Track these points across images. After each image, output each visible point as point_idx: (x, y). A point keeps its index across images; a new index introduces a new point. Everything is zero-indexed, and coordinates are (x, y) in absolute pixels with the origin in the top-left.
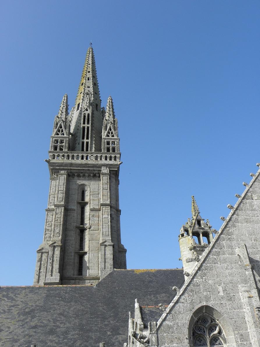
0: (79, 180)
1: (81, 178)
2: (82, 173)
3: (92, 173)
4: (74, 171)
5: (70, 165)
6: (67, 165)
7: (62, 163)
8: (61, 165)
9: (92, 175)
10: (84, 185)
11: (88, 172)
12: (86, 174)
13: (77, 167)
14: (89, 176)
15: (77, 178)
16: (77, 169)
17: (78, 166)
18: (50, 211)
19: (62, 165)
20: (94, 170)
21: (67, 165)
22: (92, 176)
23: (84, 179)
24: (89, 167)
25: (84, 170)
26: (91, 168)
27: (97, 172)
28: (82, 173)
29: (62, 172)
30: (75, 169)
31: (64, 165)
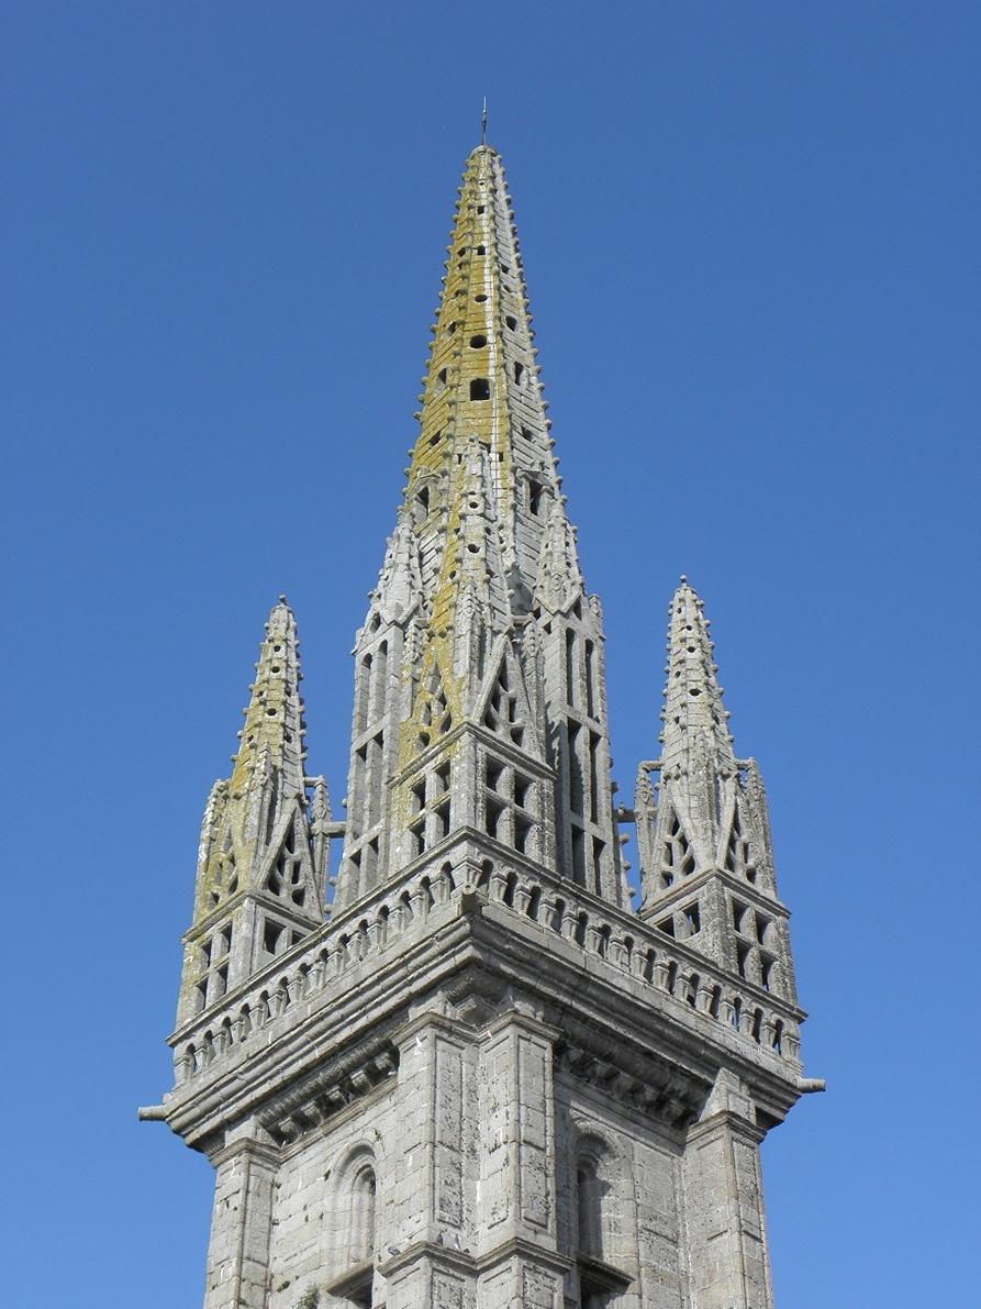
0: (582, 1097)
1: (587, 1091)
2: (608, 1058)
3: (652, 1085)
4: (579, 1030)
5: (575, 982)
6: (561, 974)
7: (542, 952)
8: (533, 958)
9: (650, 1093)
10: (594, 1145)
11: (641, 1065)
12: (625, 1080)
13: (600, 1011)
14: (635, 1091)
15: (569, 1079)
16: (595, 1025)
17: (611, 1007)
18: (444, 1261)
19: (535, 958)
20: (674, 1067)
21: (561, 974)
22: (649, 1105)
23: (603, 1099)
24: (660, 1038)
25: (627, 1042)
26: (667, 1049)
27: (681, 1086)
28: (608, 1058)
29: (524, 1007)
30: (585, 1019)
31: (546, 967)
